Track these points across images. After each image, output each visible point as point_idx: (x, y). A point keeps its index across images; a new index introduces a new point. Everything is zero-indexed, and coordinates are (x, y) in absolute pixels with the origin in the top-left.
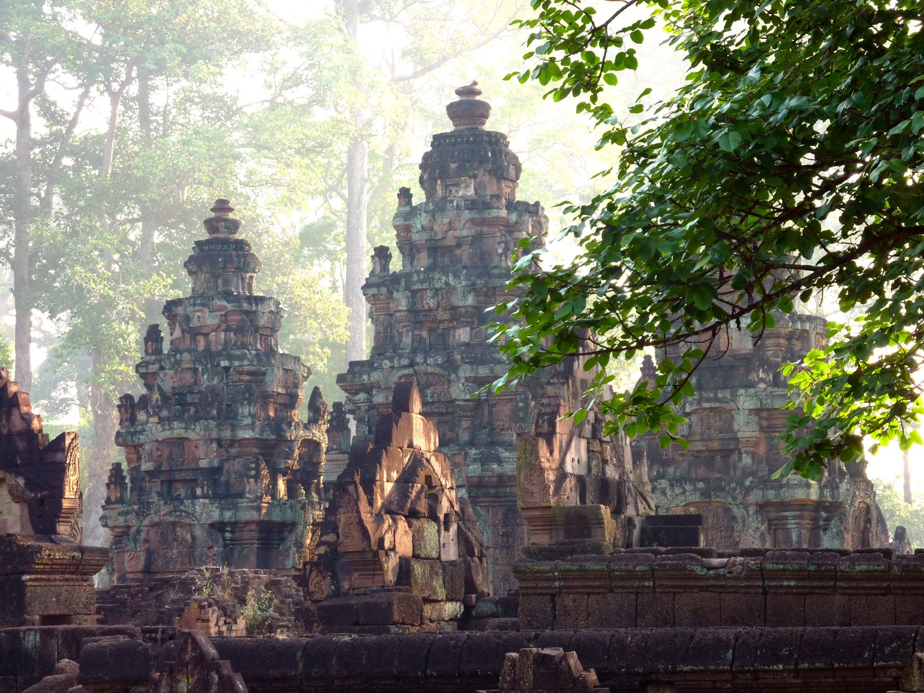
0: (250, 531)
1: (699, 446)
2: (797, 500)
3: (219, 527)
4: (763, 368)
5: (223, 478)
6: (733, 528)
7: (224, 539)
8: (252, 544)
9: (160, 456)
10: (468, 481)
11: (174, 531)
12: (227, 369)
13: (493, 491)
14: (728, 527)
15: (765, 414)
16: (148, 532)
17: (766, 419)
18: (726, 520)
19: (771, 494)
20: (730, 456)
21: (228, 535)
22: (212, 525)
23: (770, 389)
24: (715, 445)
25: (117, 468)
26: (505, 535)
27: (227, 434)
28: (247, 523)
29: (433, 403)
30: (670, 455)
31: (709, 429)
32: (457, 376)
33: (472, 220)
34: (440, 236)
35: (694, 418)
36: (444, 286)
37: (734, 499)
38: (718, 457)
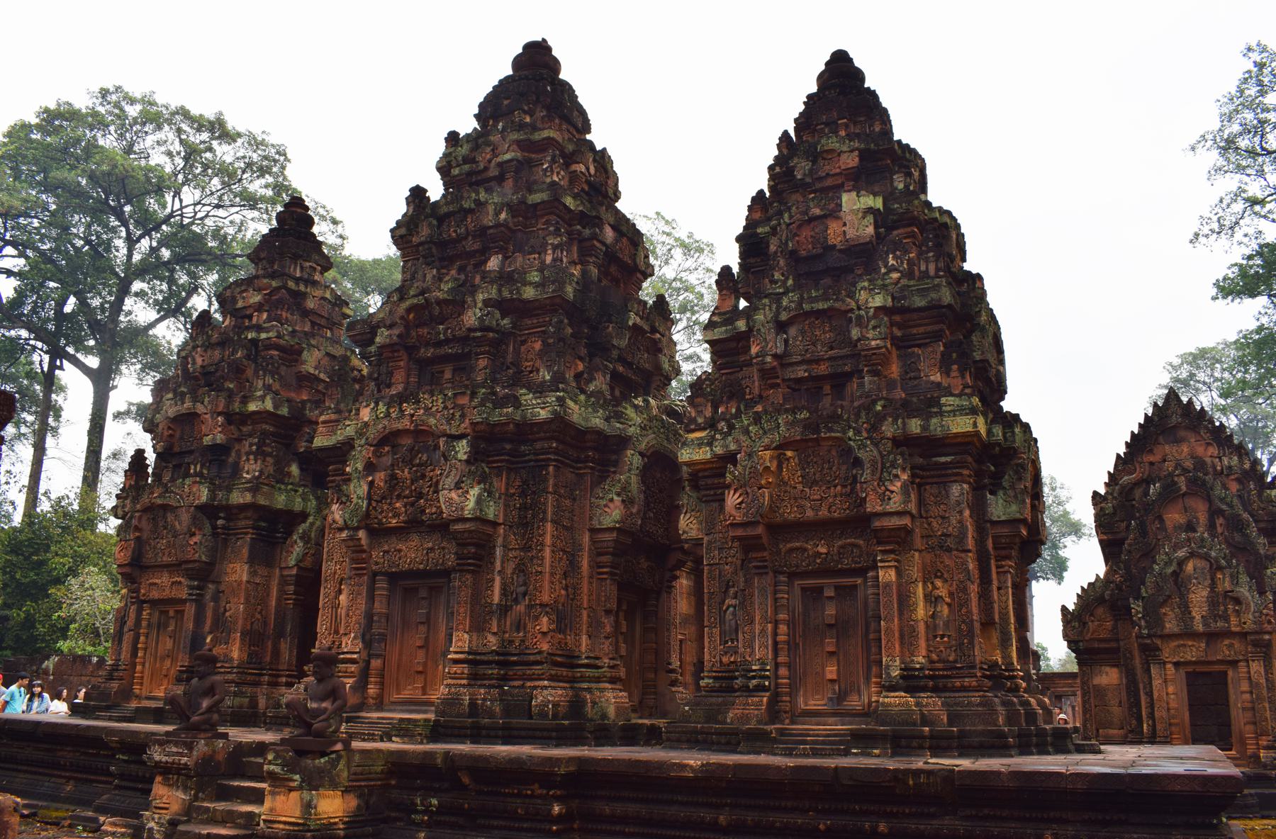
0: (246, 518)
1: (801, 373)
2: (957, 435)
3: (208, 511)
4: (893, 253)
5: (231, 460)
6: (855, 477)
7: (214, 527)
8: (247, 533)
9: (171, 436)
10: (474, 430)
11: (165, 517)
12: (254, 342)
13: (508, 447)
14: (846, 479)
15: (897, 318)
16: (140, 518)
17: (901, 326)
18: (844, 468)
19: (915, 426)
20: (844, 385)
21: (220, 522)
22: (201, 508)
23: (904, 282)
24: (823, 369)
25: (139, 454)
26: (524, 507)
27: (236, 406)
28: (243, 508)
29: (447, 341)
30: (756, 391)
31: (814, 344)
32: (475, 301)
33: (518, 142)
34: (482, 166)
35: (793, 331)
36: (473, 206)
37: (857, 432)
38: (827, 389)
